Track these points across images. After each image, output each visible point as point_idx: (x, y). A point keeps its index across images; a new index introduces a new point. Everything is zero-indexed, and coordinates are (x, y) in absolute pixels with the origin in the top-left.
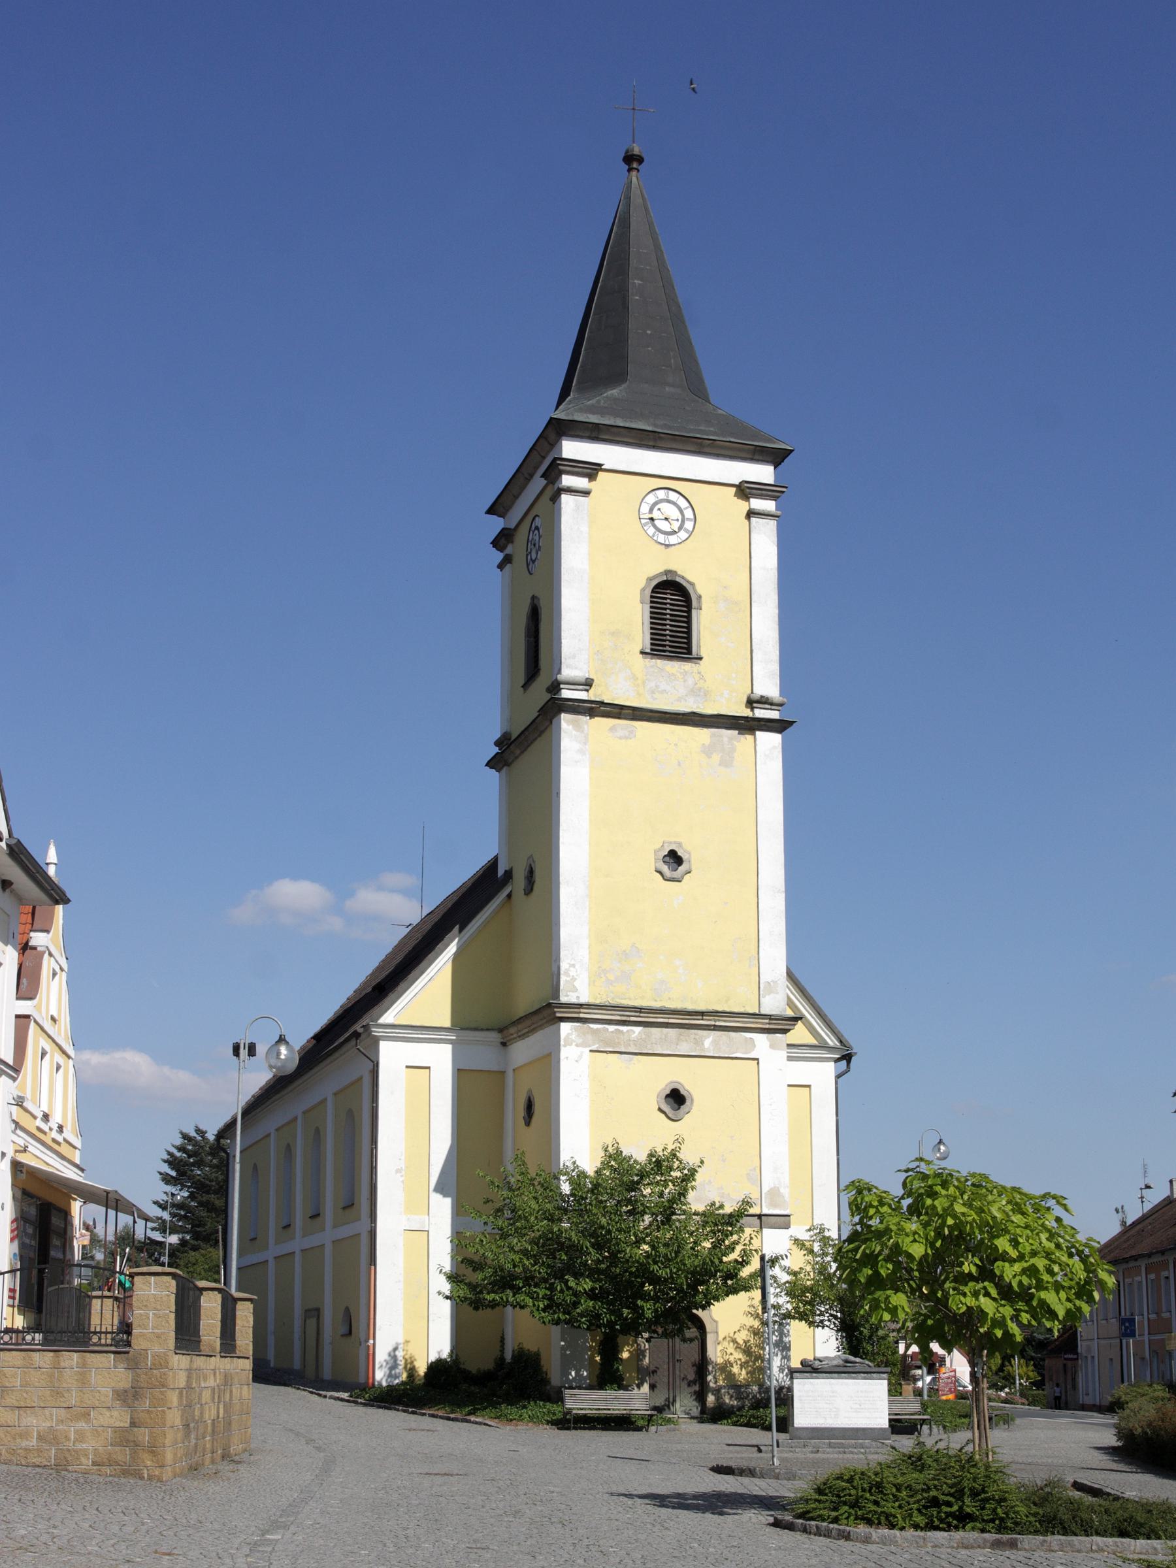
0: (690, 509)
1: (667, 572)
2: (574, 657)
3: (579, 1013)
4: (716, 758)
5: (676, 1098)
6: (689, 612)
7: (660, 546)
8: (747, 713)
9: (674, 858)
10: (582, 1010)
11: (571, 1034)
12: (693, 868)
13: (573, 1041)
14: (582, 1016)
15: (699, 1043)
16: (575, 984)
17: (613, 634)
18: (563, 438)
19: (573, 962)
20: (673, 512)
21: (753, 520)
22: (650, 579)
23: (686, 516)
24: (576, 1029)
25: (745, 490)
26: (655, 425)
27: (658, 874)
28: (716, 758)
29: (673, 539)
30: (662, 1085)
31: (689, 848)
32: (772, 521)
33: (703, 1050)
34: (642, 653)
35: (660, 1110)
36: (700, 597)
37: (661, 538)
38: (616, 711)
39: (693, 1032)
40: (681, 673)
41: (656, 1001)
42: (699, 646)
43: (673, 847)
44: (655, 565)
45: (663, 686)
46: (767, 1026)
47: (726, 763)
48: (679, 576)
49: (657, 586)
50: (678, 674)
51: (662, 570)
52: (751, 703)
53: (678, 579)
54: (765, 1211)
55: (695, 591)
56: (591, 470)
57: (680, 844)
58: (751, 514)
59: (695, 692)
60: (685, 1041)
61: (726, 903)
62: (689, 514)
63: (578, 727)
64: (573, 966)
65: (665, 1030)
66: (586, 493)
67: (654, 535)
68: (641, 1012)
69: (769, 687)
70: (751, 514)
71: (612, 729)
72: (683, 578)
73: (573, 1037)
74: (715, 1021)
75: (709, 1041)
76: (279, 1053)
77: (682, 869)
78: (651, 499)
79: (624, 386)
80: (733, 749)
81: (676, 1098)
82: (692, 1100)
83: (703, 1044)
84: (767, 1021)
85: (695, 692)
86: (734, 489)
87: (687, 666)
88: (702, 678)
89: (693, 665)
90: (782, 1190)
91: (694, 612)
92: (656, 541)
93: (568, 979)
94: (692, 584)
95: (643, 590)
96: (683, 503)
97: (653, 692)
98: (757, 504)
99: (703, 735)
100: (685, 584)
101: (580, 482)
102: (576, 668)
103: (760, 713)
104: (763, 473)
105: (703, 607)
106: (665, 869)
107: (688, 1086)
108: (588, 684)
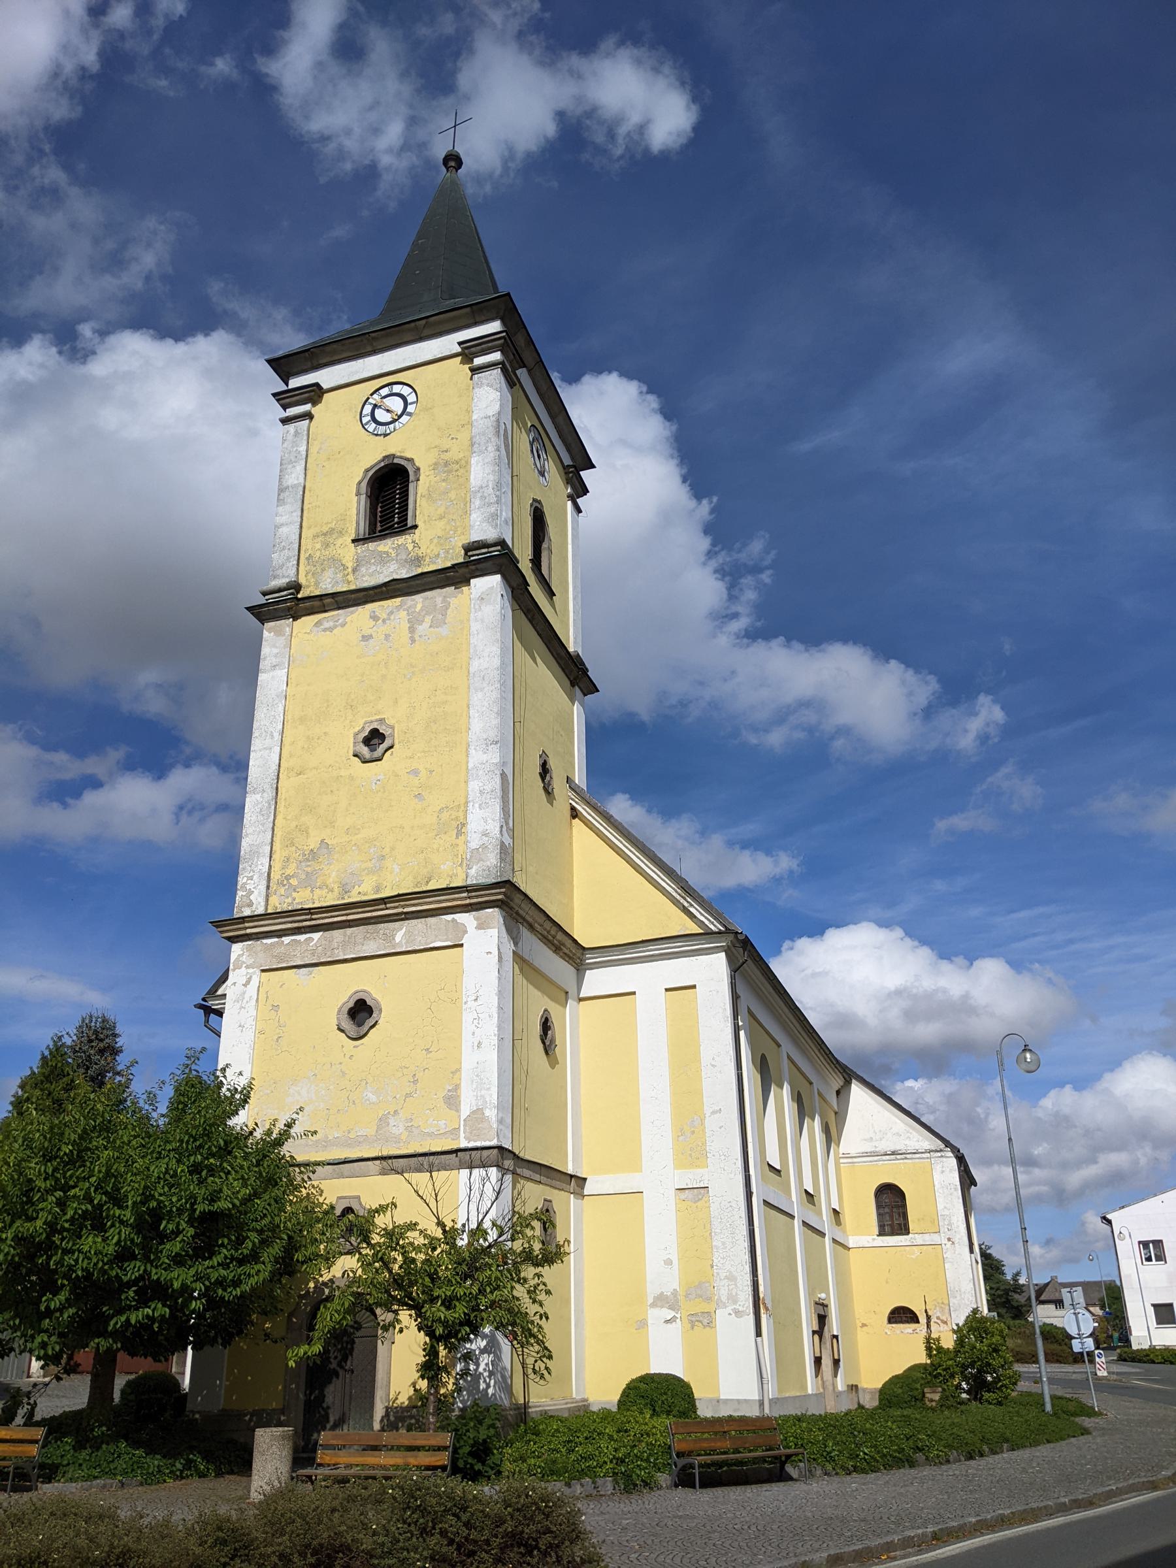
0: (394, 386)
7: (378, 438)
10: (247, 925)
11: (243, 954)
12: (396, 742)
13: (244, 962)
14: (249, 931)
15: (390, 938)
16: (252, 897)
17: (325, 534)
19: (252, 874)
22: (367, 471)
23: (409, 401)
24: (249, 949)
27: (356, 759)
30: (344, 998)
31: (390, 722)
32: (496, 371)
38: (317, 603)
40: (393, 548)
41: (343, 898)
43: (375, 725)
46: (468, 901)
48: (398, 457)
50: (391, 551)
51: (380, 457)
53: (396, 461)
58: (475, 370)
60: (365, 940)
61: (431, 772)
63: (279, 633)
64: (251, 878)
65: (349, 931)
66: (309, 416)
67: (366, 424)
68: (312, 914)
72: (401, 457)
73: (244, 958)
74: (403, 907)
75: (401, 934)
76: (1026, 1058)
82: (380, 1011)
83: (394, 939)
84: (465, 895)
86: (459, 358)
89: (407, 536)
90: (487, 1113)
92: (377, 435)
93: (244, 893)
94: (411, 460)
95: (360, 483)
96: (405, 391)
100: (402, 462)
102: (283, 577)
105: (421, 478)
106: (365, 751)
107: (376, 994)
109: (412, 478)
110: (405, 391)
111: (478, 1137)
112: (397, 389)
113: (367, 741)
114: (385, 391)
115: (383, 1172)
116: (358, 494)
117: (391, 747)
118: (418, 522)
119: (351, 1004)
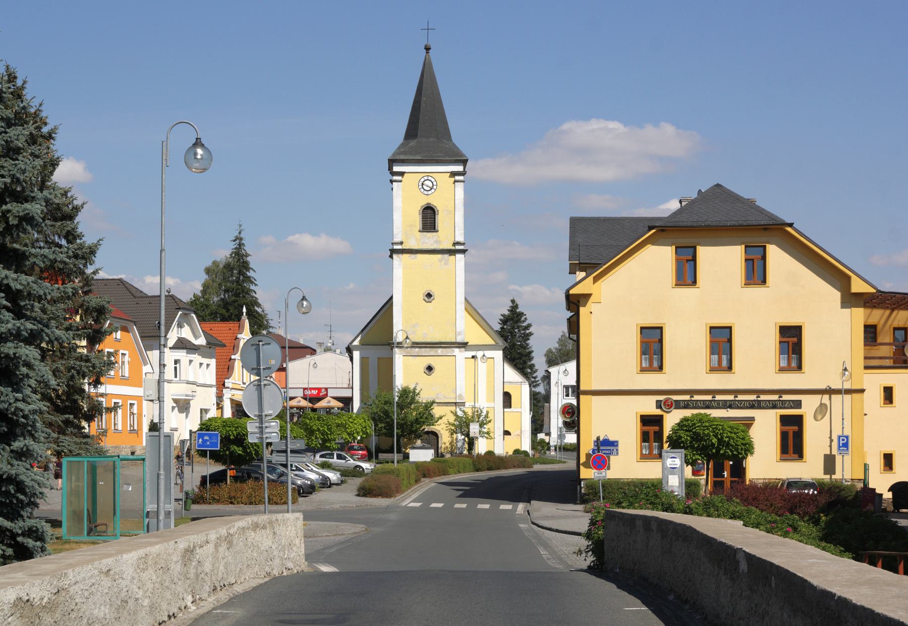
1: (428, 204)
2: (397, 234)
3: (400, 345)
4: (443, 262)
5: (430, 369)
6: (435, 215)
8: (453, 248)
9: (429, 295)
18: (394, 164)
20: (430, 185)
21: (456, 183)
22: (422, 207)
25: (453, 174)
26: (422, 157)
28: (443, 262)
29: (430, 192)
30: (425, 365)
33: (438, 353)
34: (420, 231)
35: (425, 372)
36: (438, 211)
37: (426, 192)
39: (434, 349)
42: (438, 227)
44: (423, 201)
45: (426, 241)
47: (446, 264)
49: (424, 210)
51: (426, 203)
52: (455, 244)
53: (431, 206)
54: (457, 401)
55: (437, 209)
56: (402, 174)
57: (431, 291)
58: (455, 181)
59: (436, 242)
60: (432, 352)
62: (435, 183)
63: (398, 257)
69: (460, 238)
70: (455, 181)
71: (410, 256)
75: (440, 351)
77: (432, 298)
78: (422, 180)
79: (416, 140)
80: (449, 259)
81: (430, 369)
85: (437, 242)
86: (449, 174)
87: (434, 234)
88: (439, 237)
90: (463, 395)
91: (436, 216)
94: (436, 207)
97: (423, 243)
98: (457, 178)
99: (439, 256)
100: (433, 207)
101: (399, 178)
103: (458, 247)
104: (460, 168)
106: (426, 299)
107: (433, 364)
108: (401, 243)
109: (436, 213)
110: (433, 180)
111: (461, 400)
112: (430, 178)
113: (426, 296)
114: (426, 178)
115: (438, 406)
116: (419, 214)
117: (434, 299)
118: (439, 229)
119: (427, 366)
